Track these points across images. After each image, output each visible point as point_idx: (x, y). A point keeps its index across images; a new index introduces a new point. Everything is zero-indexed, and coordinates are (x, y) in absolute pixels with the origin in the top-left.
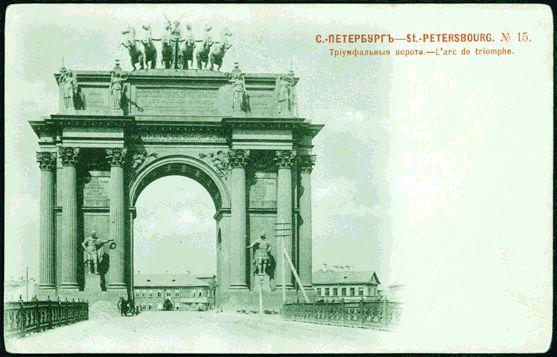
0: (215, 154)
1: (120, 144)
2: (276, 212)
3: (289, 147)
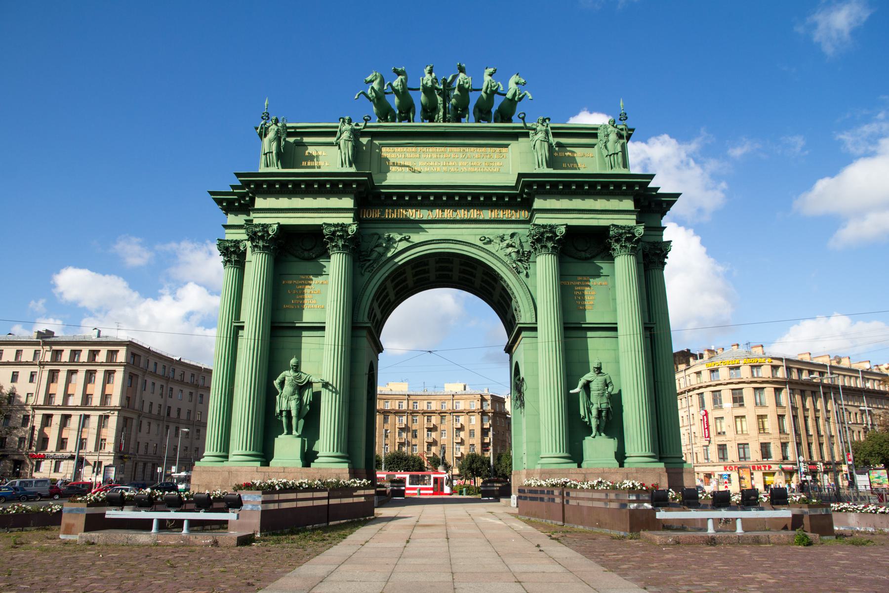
0: (507, 237)
1: (347, 219)
2: (615, 329)
3: (630, 221)
